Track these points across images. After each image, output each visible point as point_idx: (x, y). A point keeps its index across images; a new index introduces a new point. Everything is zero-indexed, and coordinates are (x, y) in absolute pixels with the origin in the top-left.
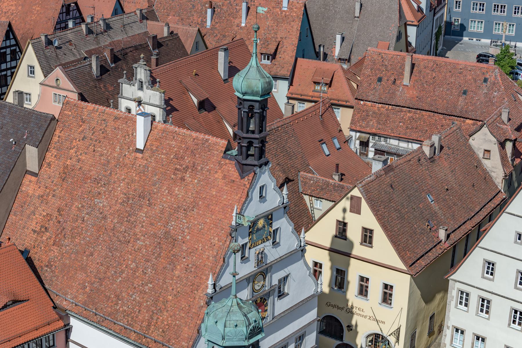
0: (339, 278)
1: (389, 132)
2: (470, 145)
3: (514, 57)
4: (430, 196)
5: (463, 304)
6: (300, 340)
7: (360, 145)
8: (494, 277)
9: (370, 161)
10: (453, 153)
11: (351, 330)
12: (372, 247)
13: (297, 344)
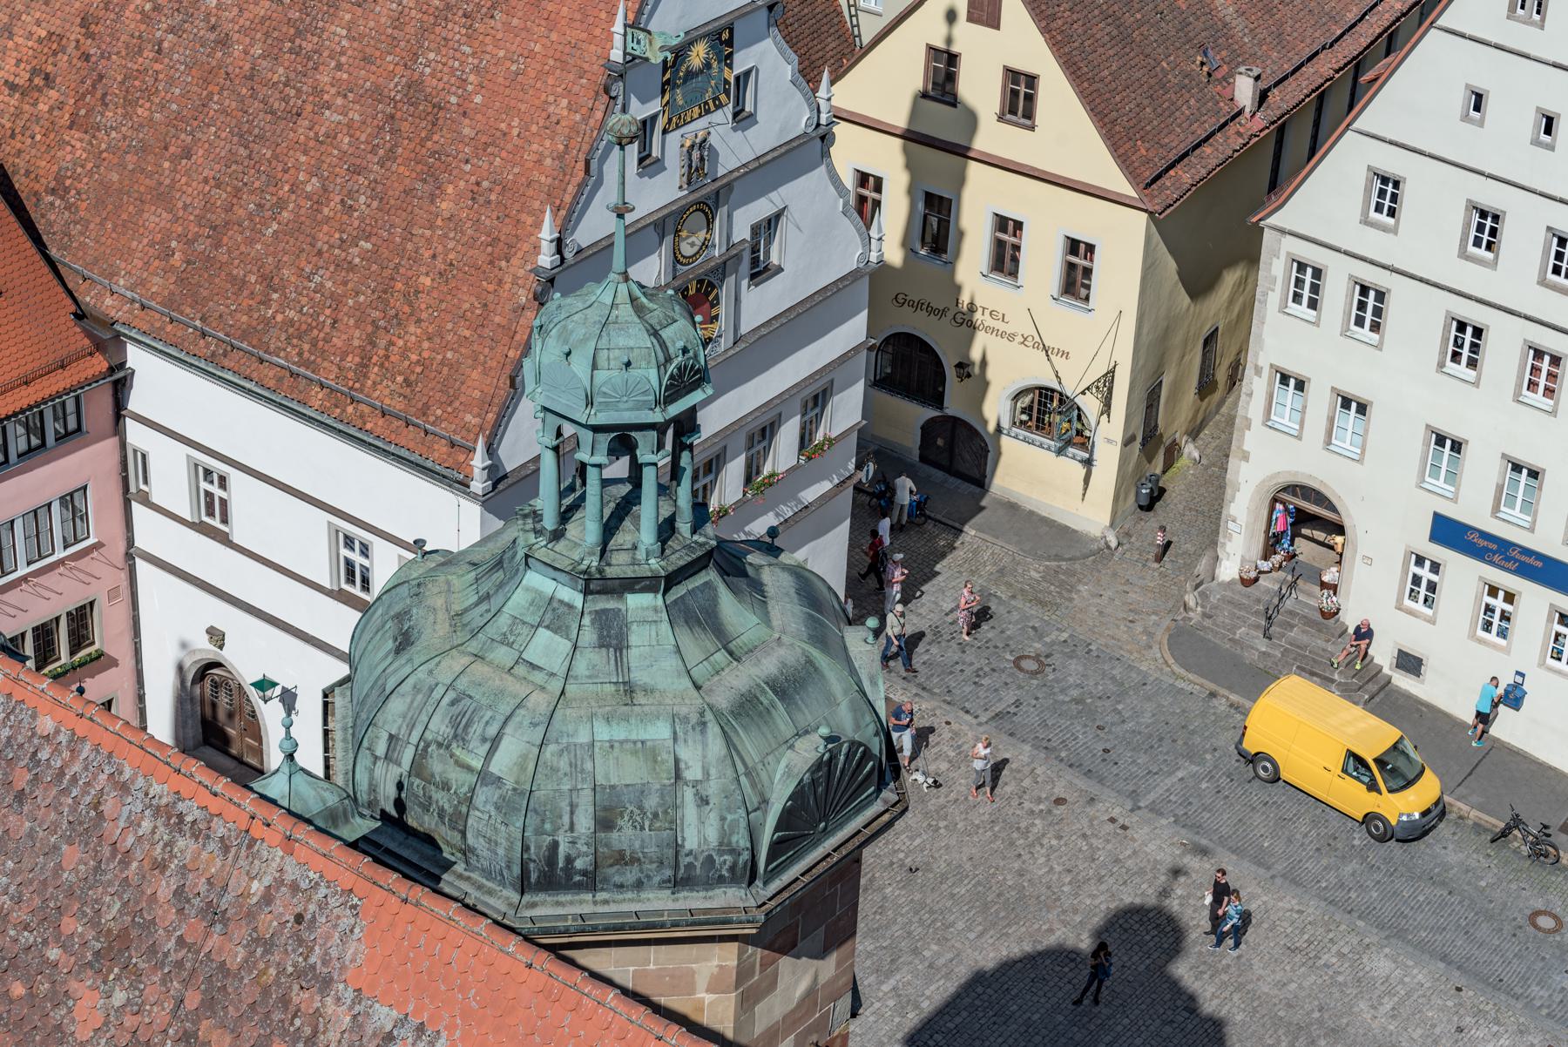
0: (934, 221)
8: (1397, 222)
11: (969, 376)
12: (1032, 128)
13: (807, 418)
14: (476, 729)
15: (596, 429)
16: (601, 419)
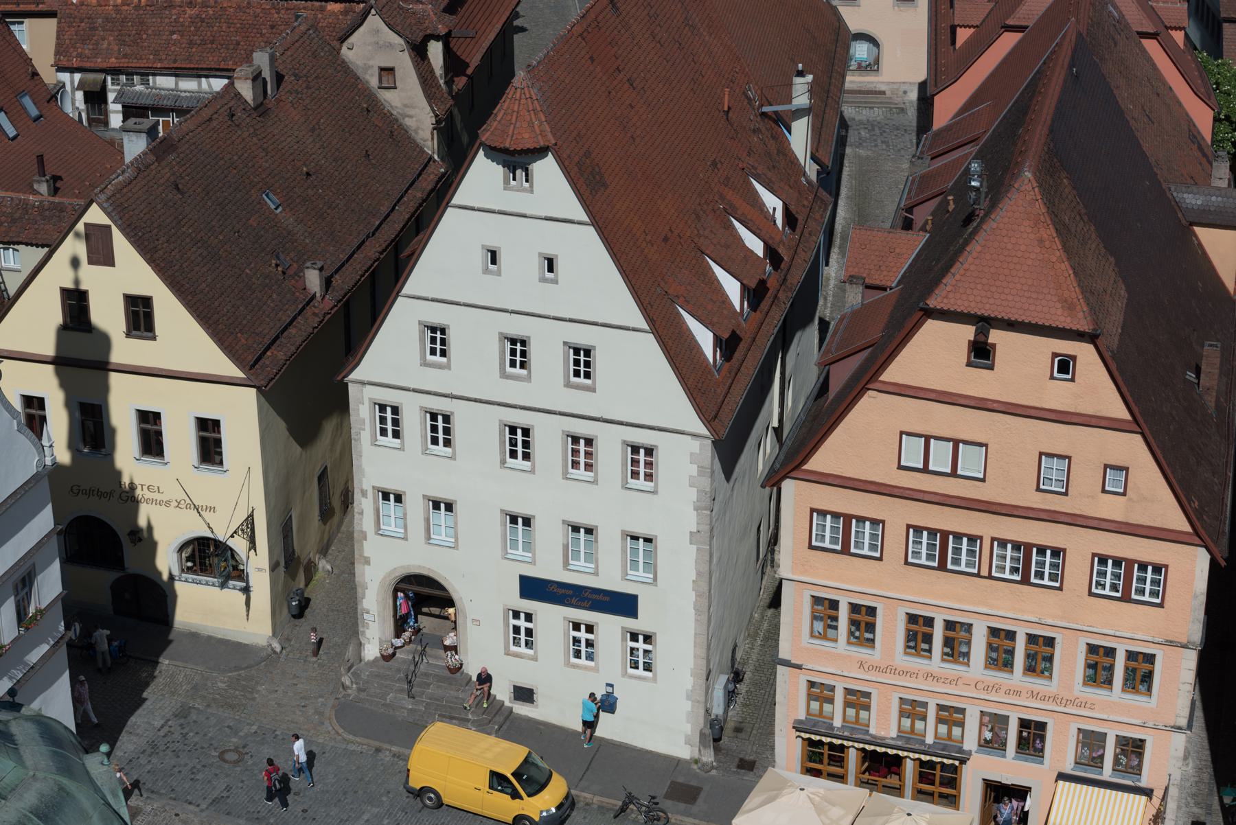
0: (90, 424)
2: (343, 62)
4: (271, 195)
5: (390, 433)
6: (24, 586)
7: (86, 102)
8: (449, 360)
9: (116, 135)
10: (308, 88)
11: (140, 540)
12: (154, 338)
13: (19, 597)
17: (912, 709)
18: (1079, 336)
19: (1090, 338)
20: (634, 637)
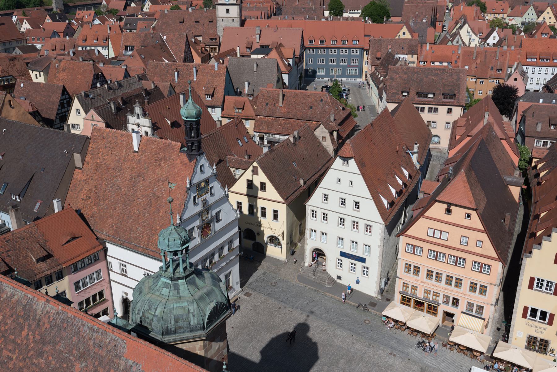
1: (274, 131)
3: (341, 86)
14: (153, 307)
15: (170, 252)
16: (171, 250)
17: (427, 292)
18: (473, 209)
19: (475, 210)
20: (365, 268)
